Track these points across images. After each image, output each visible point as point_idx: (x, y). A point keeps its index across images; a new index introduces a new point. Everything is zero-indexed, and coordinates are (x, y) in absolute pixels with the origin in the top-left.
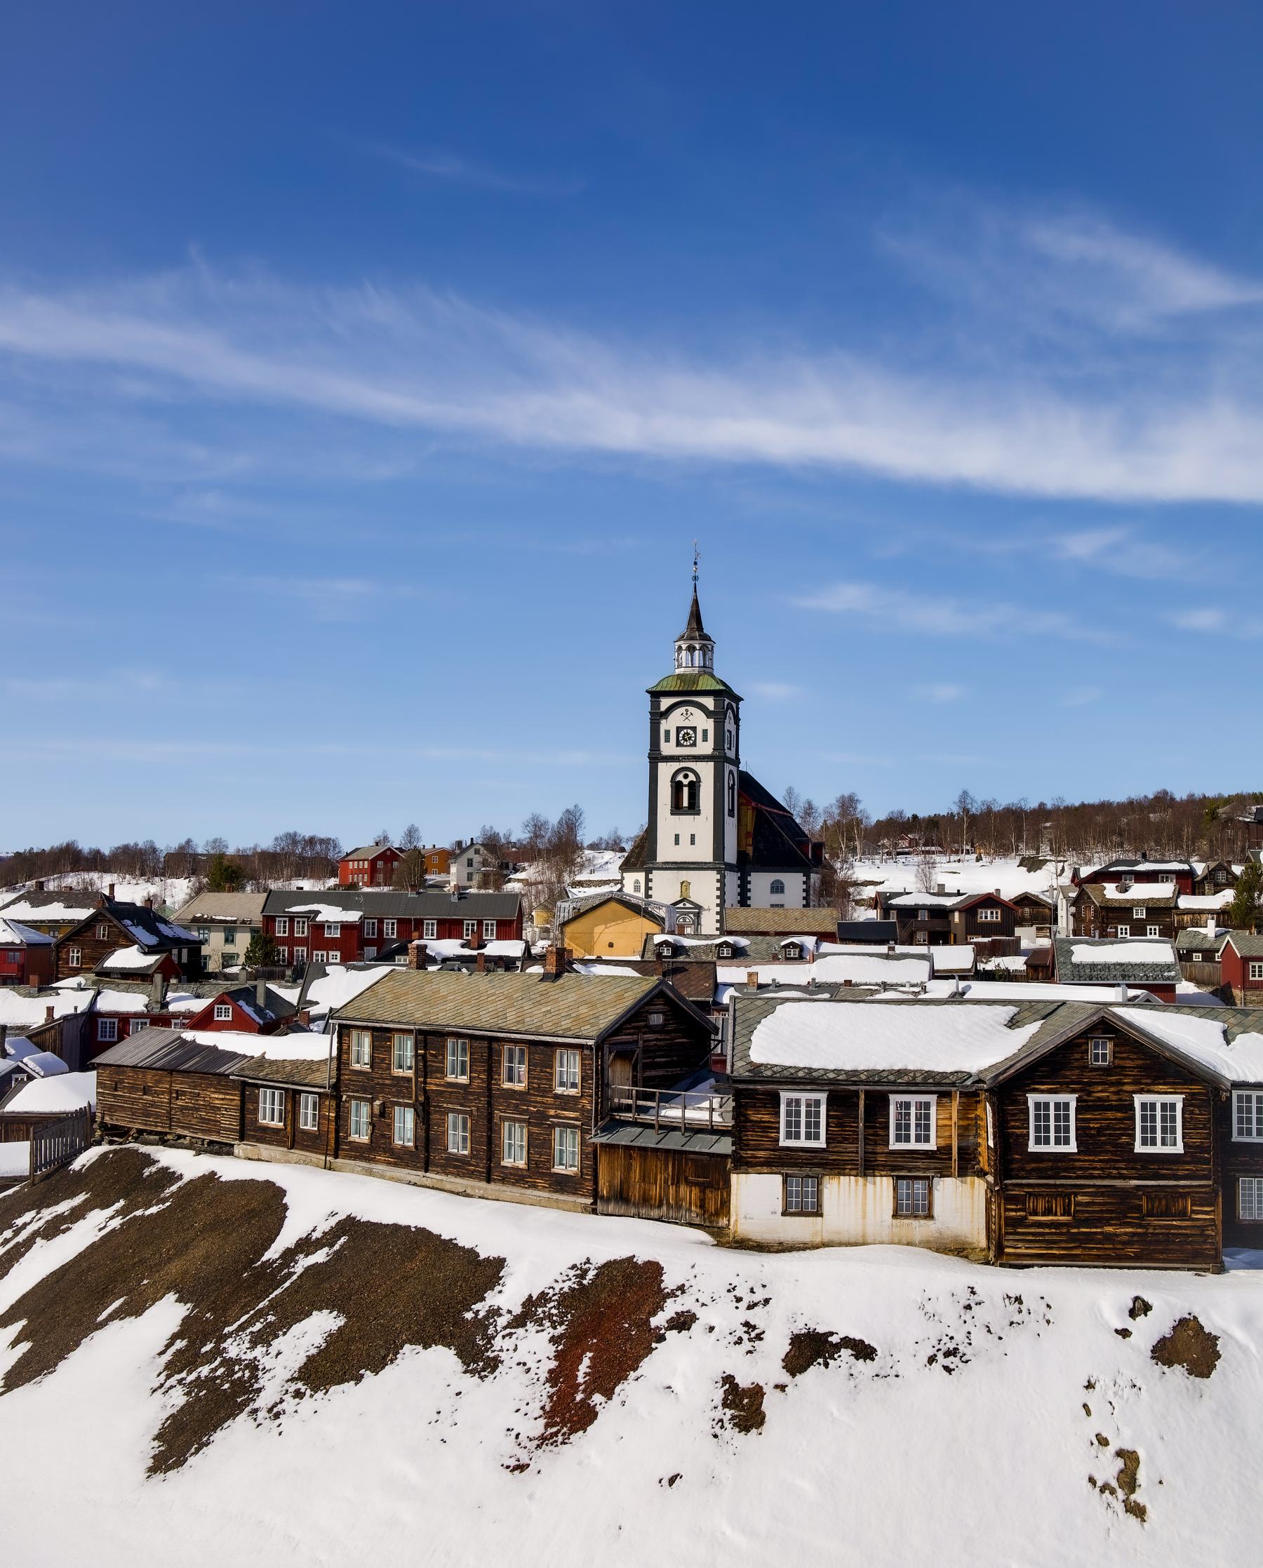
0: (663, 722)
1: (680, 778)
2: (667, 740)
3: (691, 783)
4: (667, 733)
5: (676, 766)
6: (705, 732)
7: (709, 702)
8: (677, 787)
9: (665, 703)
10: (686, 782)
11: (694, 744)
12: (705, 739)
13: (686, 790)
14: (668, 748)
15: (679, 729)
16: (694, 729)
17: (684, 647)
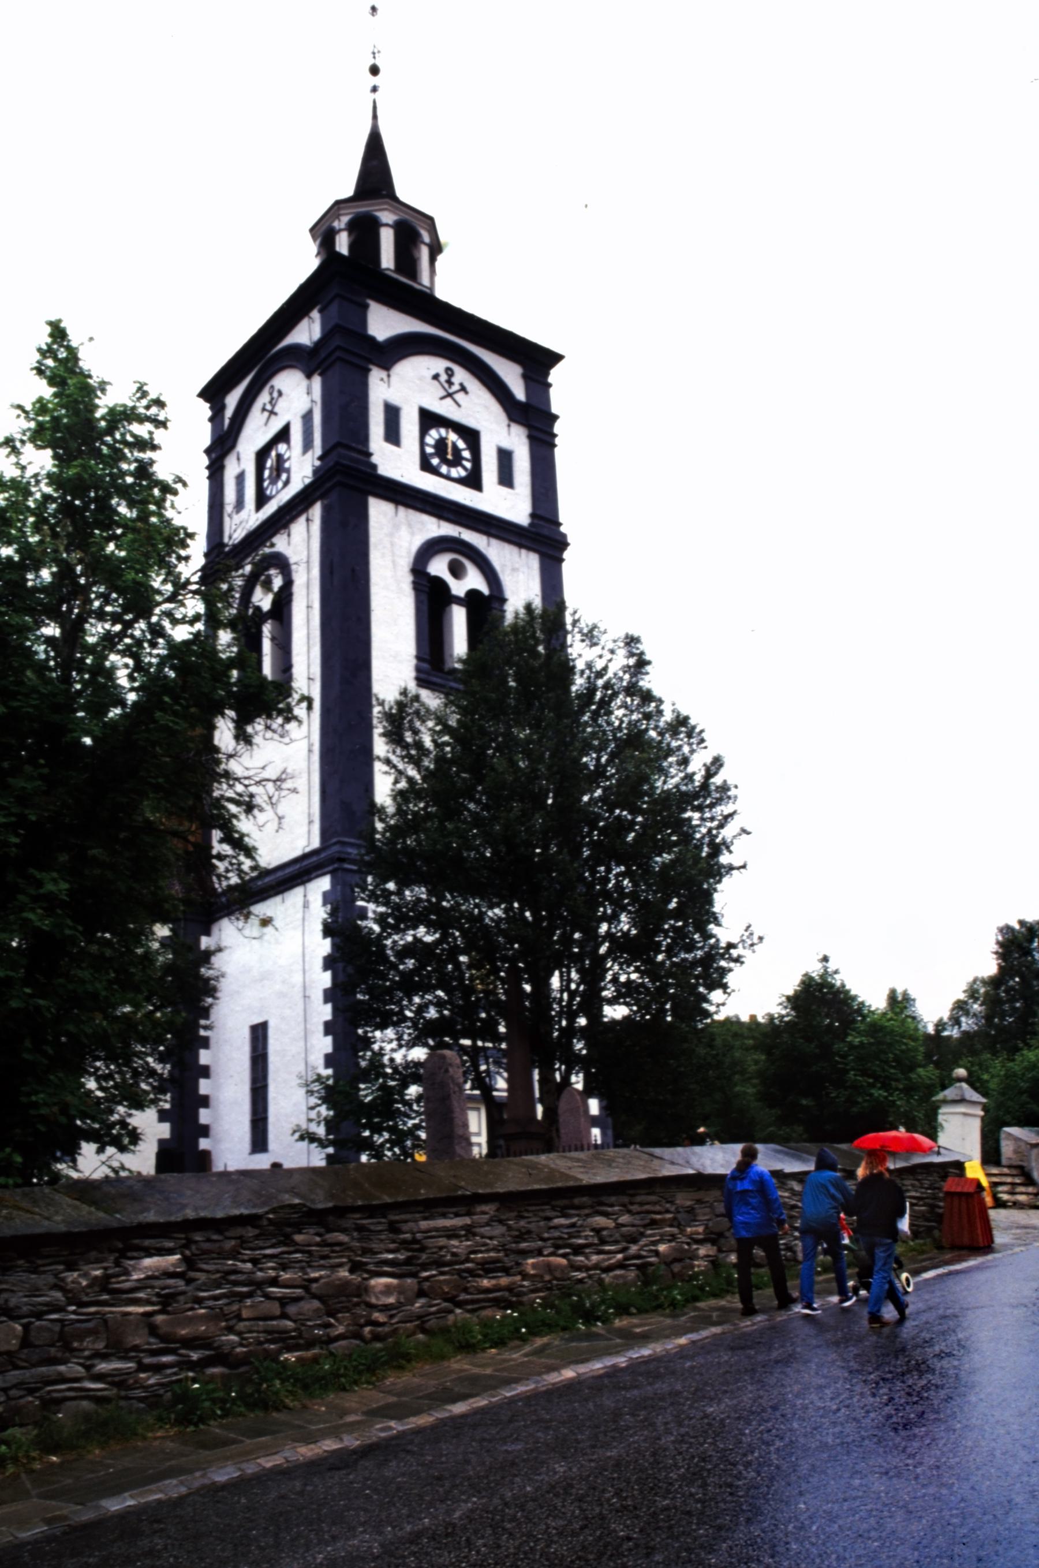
0: (376, 375)
1: (439, 567)
2: (393, 435)
4: (392, 414)
5: (435, 528)
6: (505, 457)
10: (459, 588)
11: (473, 481)
12: (506, 478)
13: (459, 617)
14: (397, 461)
15: (429, 419)
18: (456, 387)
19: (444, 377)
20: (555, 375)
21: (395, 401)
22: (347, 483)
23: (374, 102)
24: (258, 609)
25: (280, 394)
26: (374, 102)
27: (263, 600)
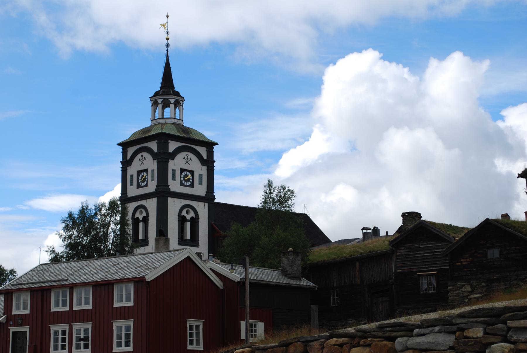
1: (184, 213)
3: (192, 218)
6: (201, 176)
7: (203, 151)
8: (182, 220)
9: (173, 146)
10: (188, 217)
11: (192, 186)
12: (200, 183)
13: (188, 224)
14: (174, 186)
15: (182, 170)
16: (192, 172)
17: (160, 101)
18: (189, 159)
19: (186, 157)
20: (215, 147)
21: (174, 168)
22: (163, 194)
23: (167, 50)
24: (138, 218)
25: (145, 159)
26: (167, 50)
27: (140, 216)
